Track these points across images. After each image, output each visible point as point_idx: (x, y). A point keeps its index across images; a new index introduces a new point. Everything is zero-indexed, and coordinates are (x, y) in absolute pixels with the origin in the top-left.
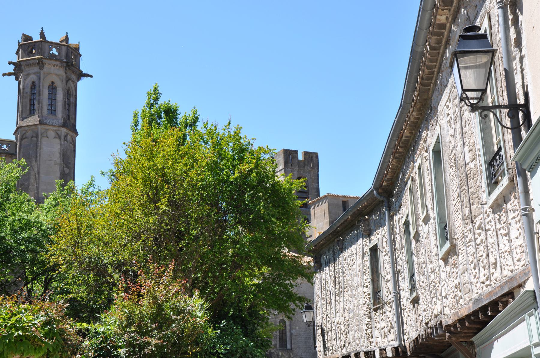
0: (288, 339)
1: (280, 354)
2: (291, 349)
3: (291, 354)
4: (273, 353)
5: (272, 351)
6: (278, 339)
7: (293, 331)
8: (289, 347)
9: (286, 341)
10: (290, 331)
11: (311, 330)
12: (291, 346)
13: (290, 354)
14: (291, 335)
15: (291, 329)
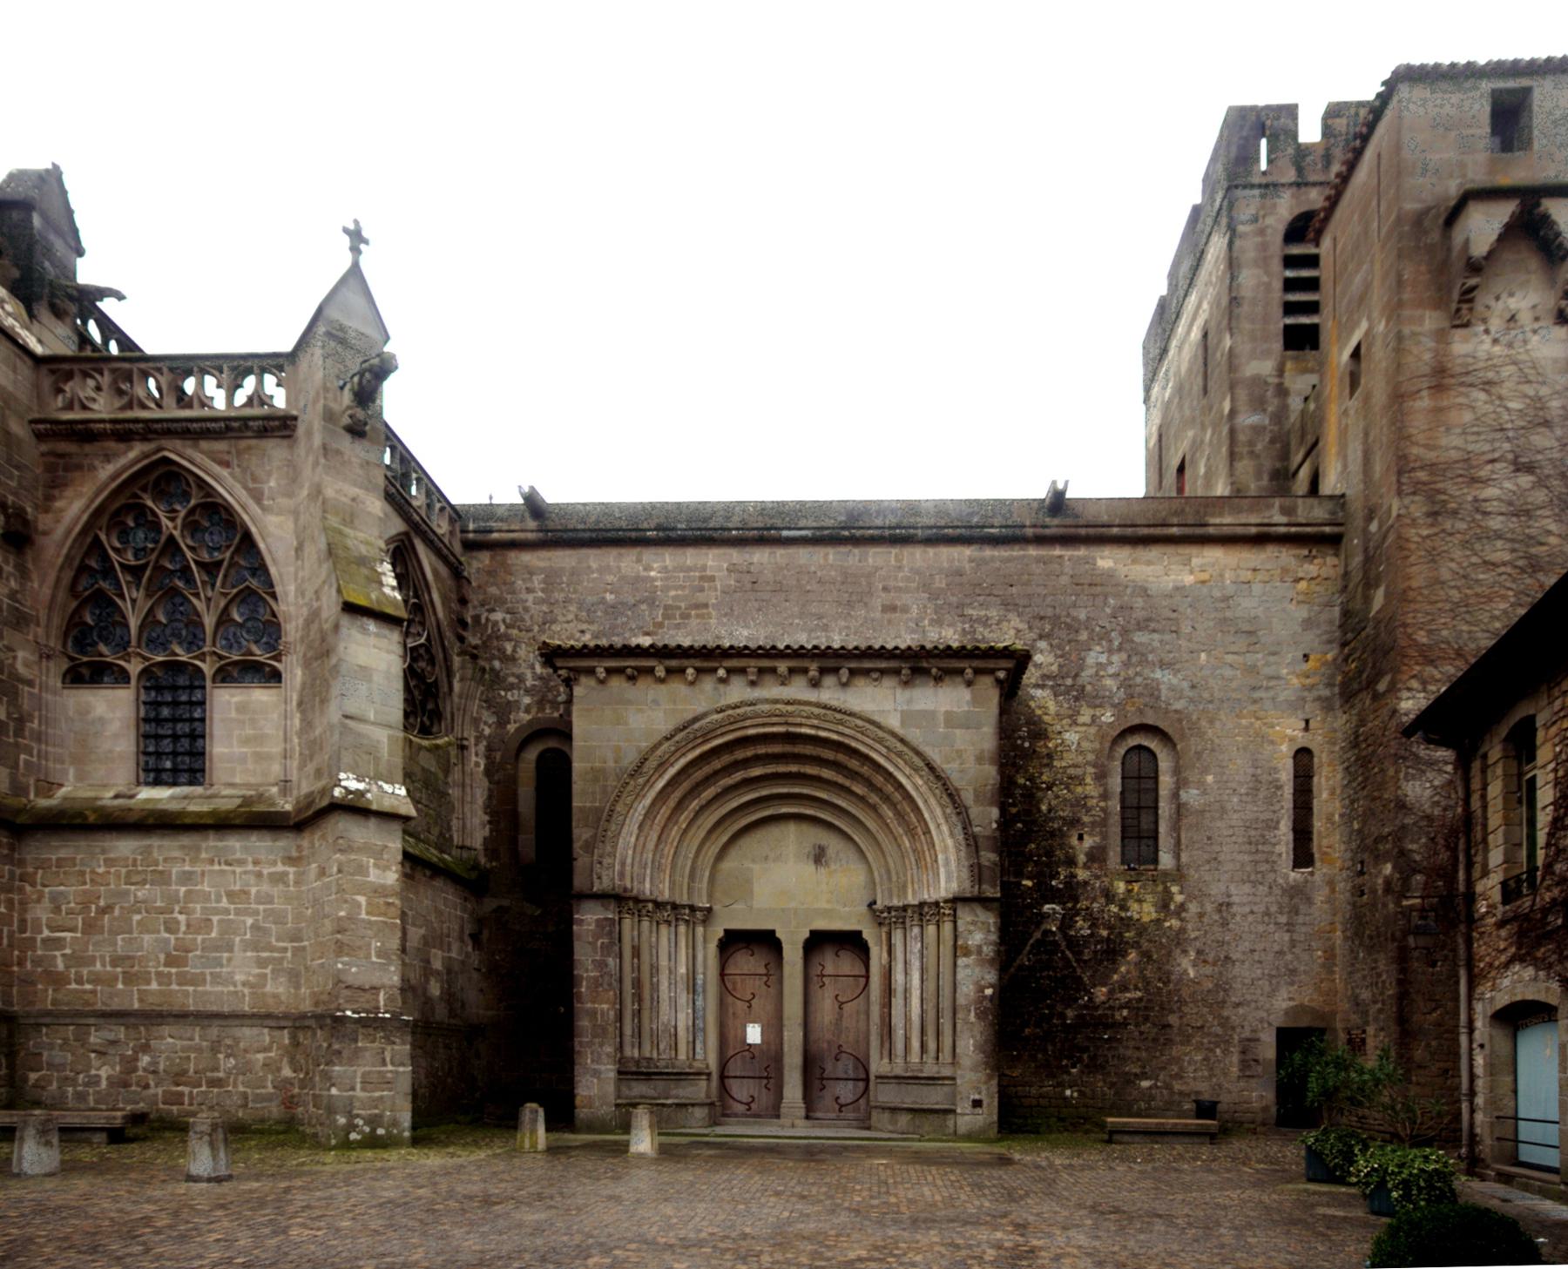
0: (1163, 828)
1: (1121, 887)
2: (1179, 868)
3: (1174, 889)
4: (1086, 883)
5: (1082, 875)
6: (1115, 830)
7: (1191, 796)
8: (1166, 860)
9: (1156, 838)
10: (1175, 795)
11: (1279, 788)
12: (1177, 857)
13: (1167, 890)
14: (1180, 809)
15: (1181, 783)
